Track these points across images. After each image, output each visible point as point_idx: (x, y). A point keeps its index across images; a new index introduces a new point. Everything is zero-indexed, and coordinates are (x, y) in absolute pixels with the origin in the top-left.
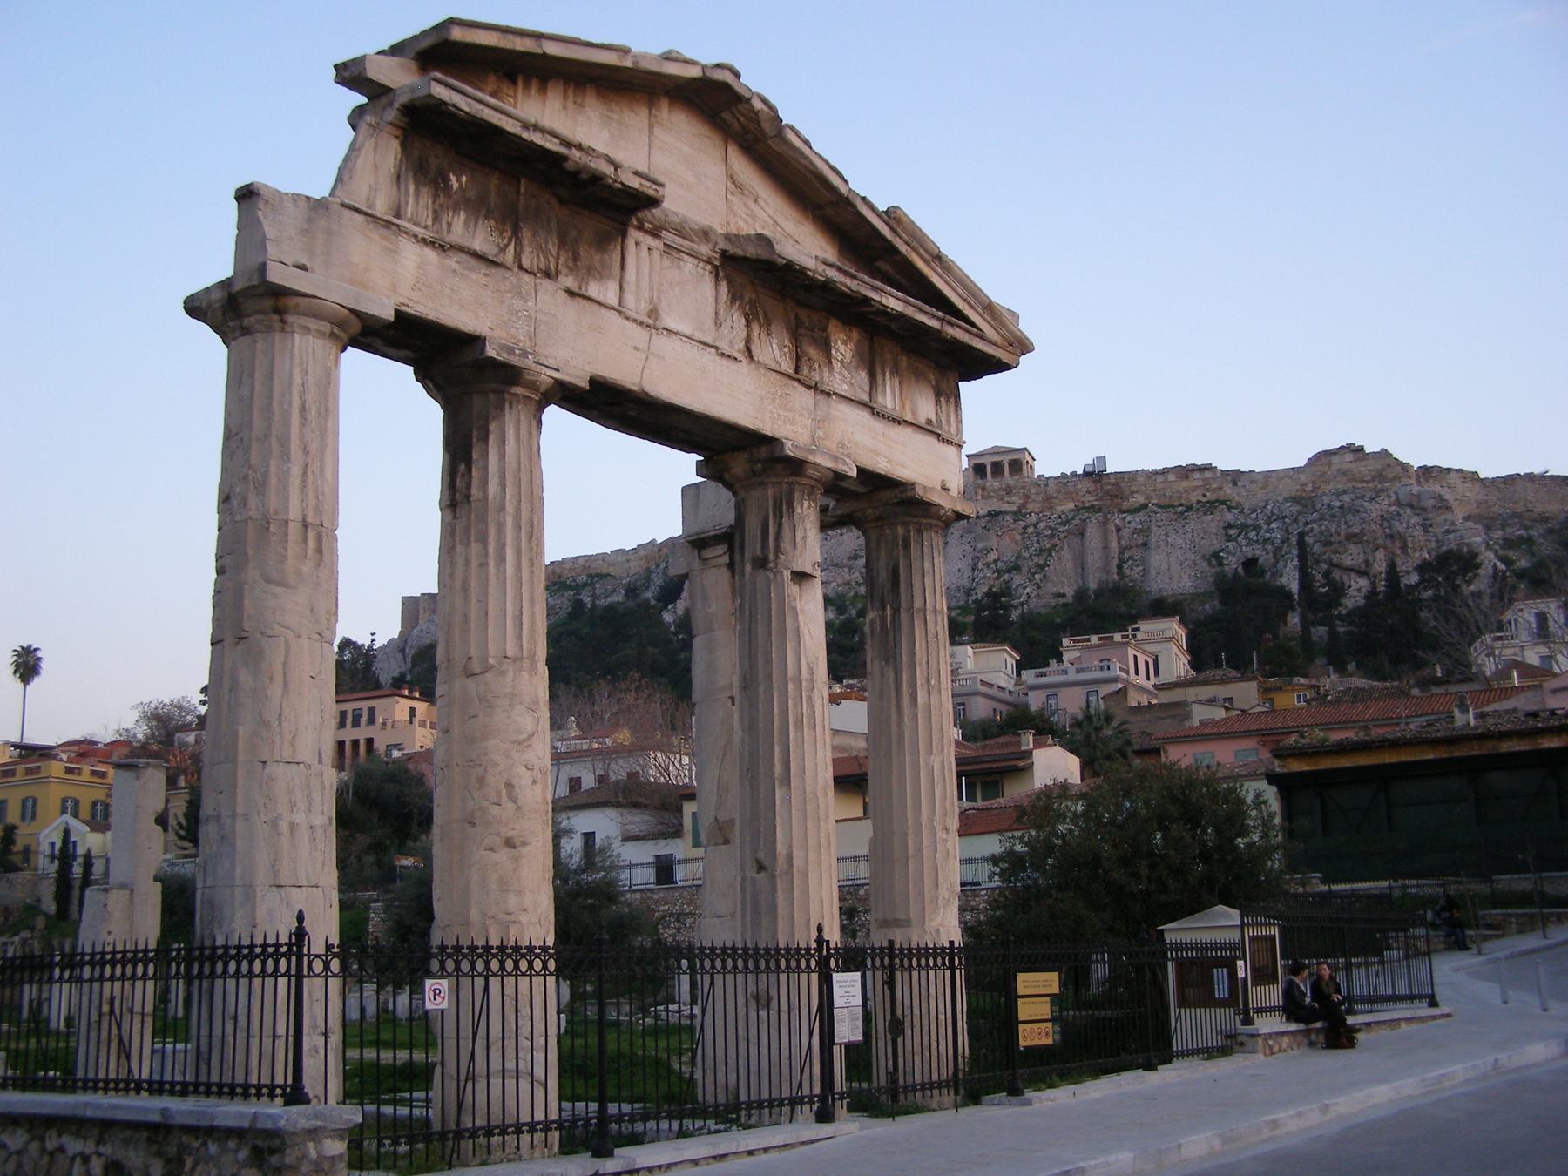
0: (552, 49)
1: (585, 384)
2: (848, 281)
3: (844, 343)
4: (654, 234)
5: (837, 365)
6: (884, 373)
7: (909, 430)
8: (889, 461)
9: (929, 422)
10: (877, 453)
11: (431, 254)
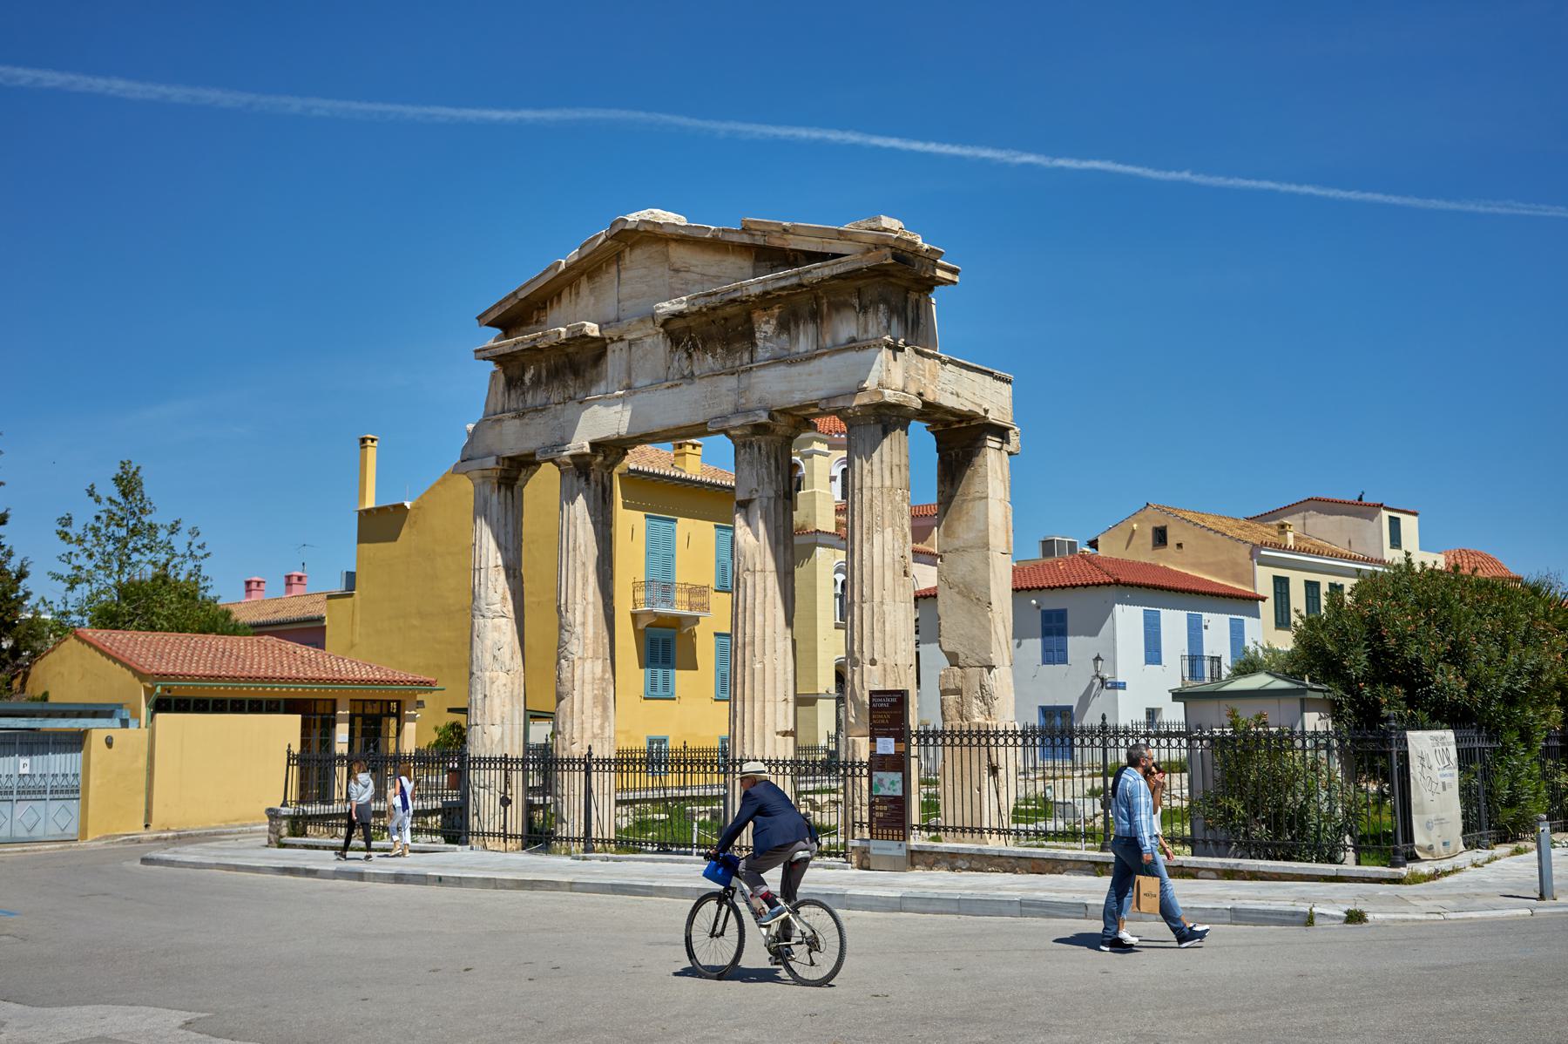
0: (522, 295)
1: (587, 449)
2: (713, 299)
3: (767, 322)
4: (621, 339)
5: (760, 343)
6: (797, 326)
7: (825, 358)
8: (804, 391)
9: (854, 340)
10: (792, 391)
11: (517, 422)
